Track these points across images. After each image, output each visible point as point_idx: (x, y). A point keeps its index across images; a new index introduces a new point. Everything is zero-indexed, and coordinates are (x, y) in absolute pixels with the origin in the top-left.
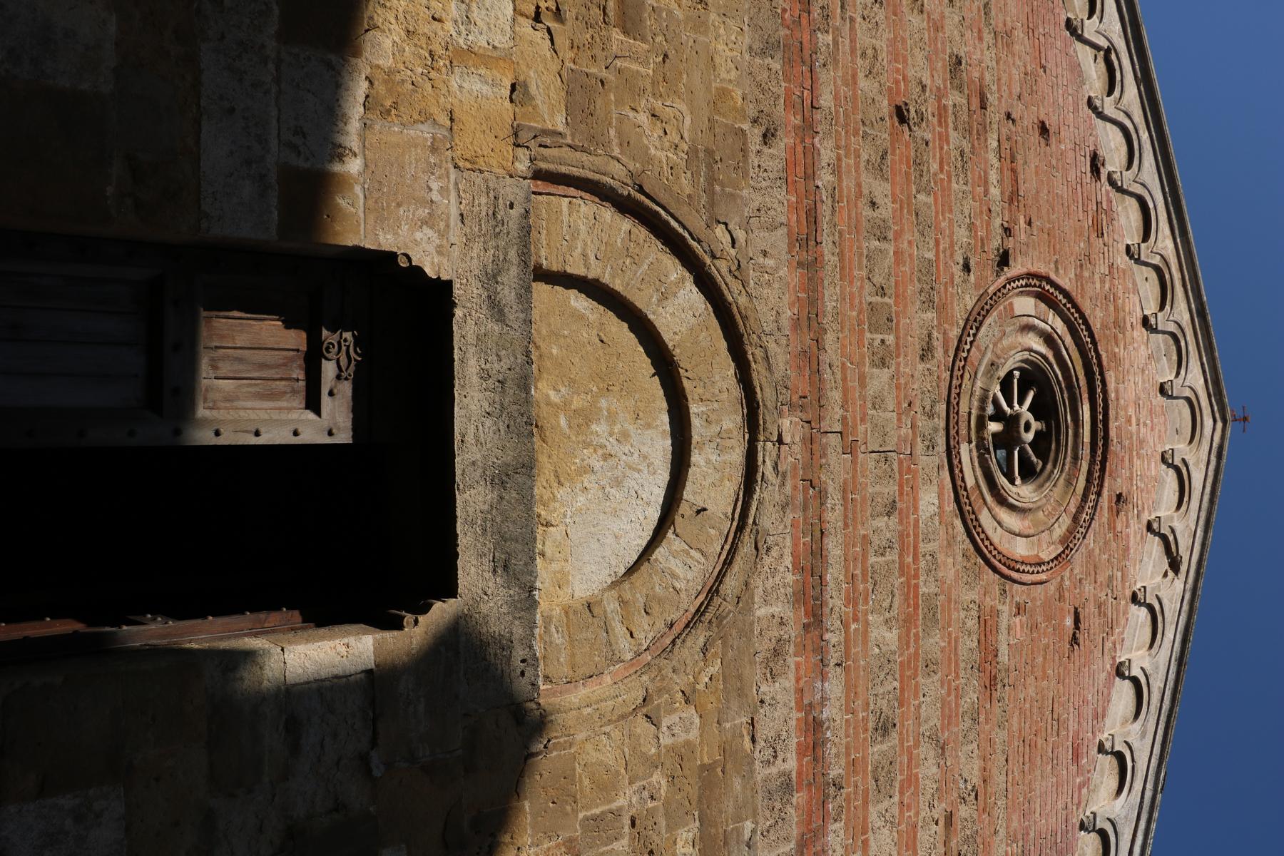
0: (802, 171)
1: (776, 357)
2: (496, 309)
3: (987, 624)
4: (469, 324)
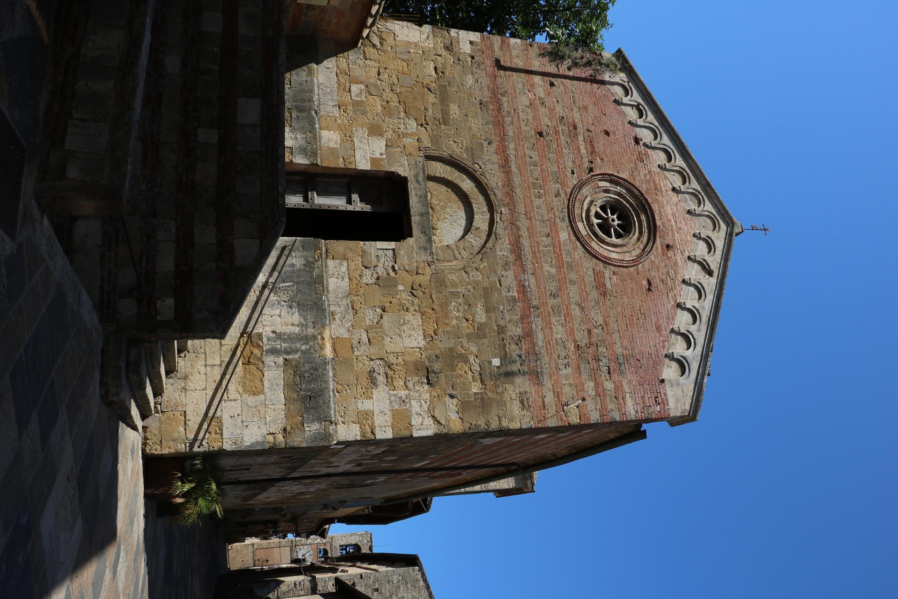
0: (502, 150)
1: (498, 195)
4: (412, 186)
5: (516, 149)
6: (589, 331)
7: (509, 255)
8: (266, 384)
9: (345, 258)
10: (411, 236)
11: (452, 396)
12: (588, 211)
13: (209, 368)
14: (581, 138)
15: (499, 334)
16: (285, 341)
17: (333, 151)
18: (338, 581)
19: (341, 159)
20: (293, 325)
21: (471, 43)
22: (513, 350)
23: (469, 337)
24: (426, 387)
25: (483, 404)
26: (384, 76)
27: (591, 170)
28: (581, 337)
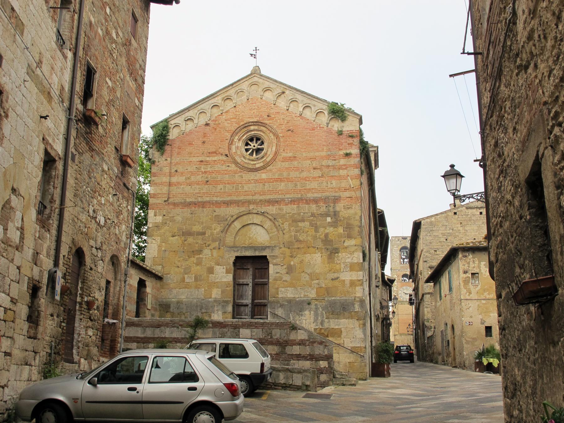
2: (238, 251)
3: (285, 160)
5: (217, 196)
6: (314, 169)
8: (337, 327)
9: (278, 289)
10: (266, 256)
11: (344, 242)
12: (249, 160)
14: (208, 159)
15: (315, 217)
16: (317, 318)
17: (223, 292)
18: (428, 281)
21: (155, 216)
22: (323, 209)
24: (340, 254)
25: (349, 227)
26: (179, 264)
27: (227, 155)
28: (317, 173)
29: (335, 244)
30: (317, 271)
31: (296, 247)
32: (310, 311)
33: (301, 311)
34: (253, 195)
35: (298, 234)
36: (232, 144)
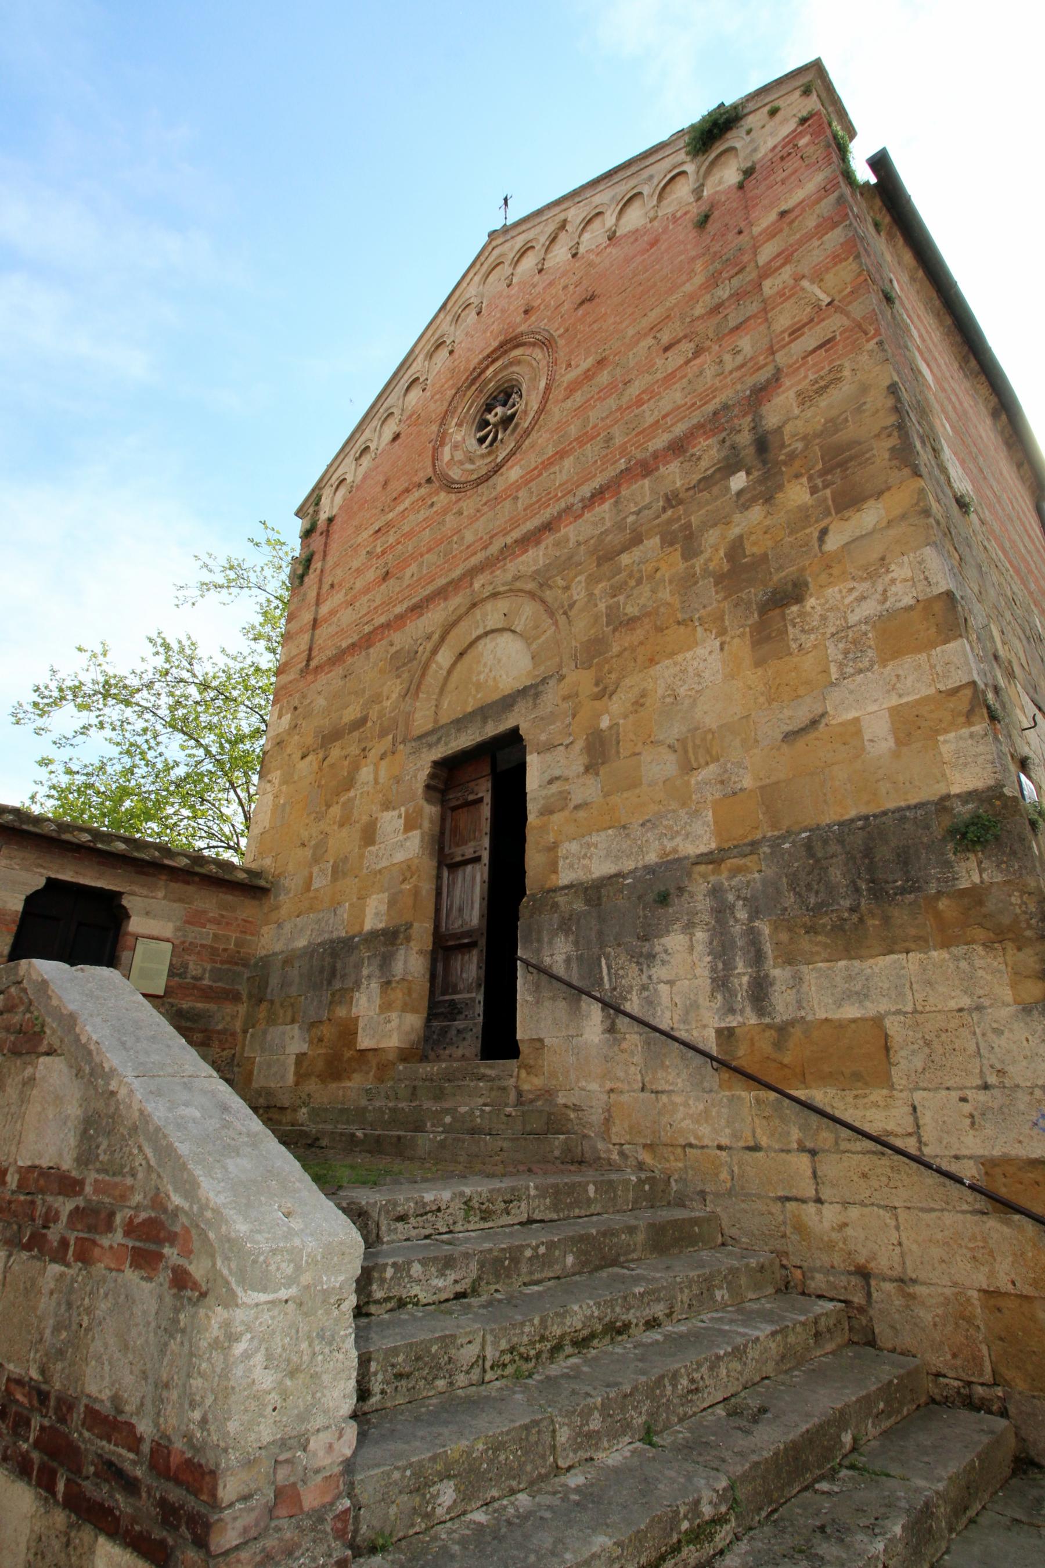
3: (572, 389)
7: (543, 546)
8: (851, 1012)
9: (553, 847)
13: (826, 1193)
15: (681, 502)
16: (729, 966)
19: (403, 886)
20: (691, 948)
23: (690, 553)
24: (811, 602)
28: (675, 359)
29: (780, 568)
30: (711, 722)
31: (616, 649)
32: (689, 927)
33: (645, 938)
34: (485, 548)
35: (621, 598)
36: (442, 444)
